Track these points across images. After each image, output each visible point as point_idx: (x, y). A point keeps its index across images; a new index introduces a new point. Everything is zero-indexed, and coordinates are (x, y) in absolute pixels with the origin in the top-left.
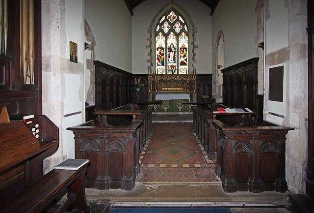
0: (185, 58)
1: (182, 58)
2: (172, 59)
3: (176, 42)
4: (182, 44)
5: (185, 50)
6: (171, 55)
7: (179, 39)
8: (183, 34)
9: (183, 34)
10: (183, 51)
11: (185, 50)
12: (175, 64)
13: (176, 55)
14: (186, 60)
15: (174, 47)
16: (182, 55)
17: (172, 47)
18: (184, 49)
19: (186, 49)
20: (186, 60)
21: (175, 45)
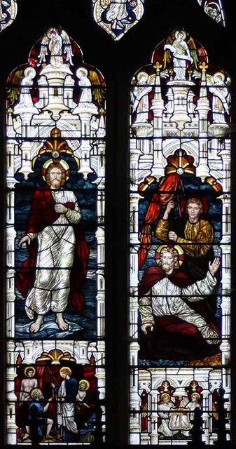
0: (203, 287)
1: (163, 287)
2: (59, 303)
3: (99, 127)
4: (171, 146)
5: (194, 208)
6: (44, 260)
7: (139, 96)
8: (179, 47)
9: (179, 47)
10: (178, 222)
11: (194, 208)
12: (81, 352)
13: (100, 256)
14: (207, 307)
15: (73, 180)
16: (167, 259)
17: (55, 176)
18: (182, 198)
19: (208, 195)
20: (207, 307)
21: (92, 164)
